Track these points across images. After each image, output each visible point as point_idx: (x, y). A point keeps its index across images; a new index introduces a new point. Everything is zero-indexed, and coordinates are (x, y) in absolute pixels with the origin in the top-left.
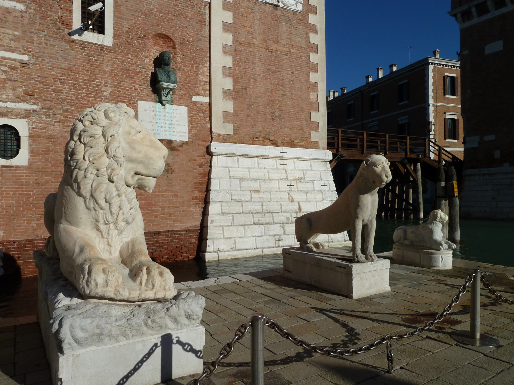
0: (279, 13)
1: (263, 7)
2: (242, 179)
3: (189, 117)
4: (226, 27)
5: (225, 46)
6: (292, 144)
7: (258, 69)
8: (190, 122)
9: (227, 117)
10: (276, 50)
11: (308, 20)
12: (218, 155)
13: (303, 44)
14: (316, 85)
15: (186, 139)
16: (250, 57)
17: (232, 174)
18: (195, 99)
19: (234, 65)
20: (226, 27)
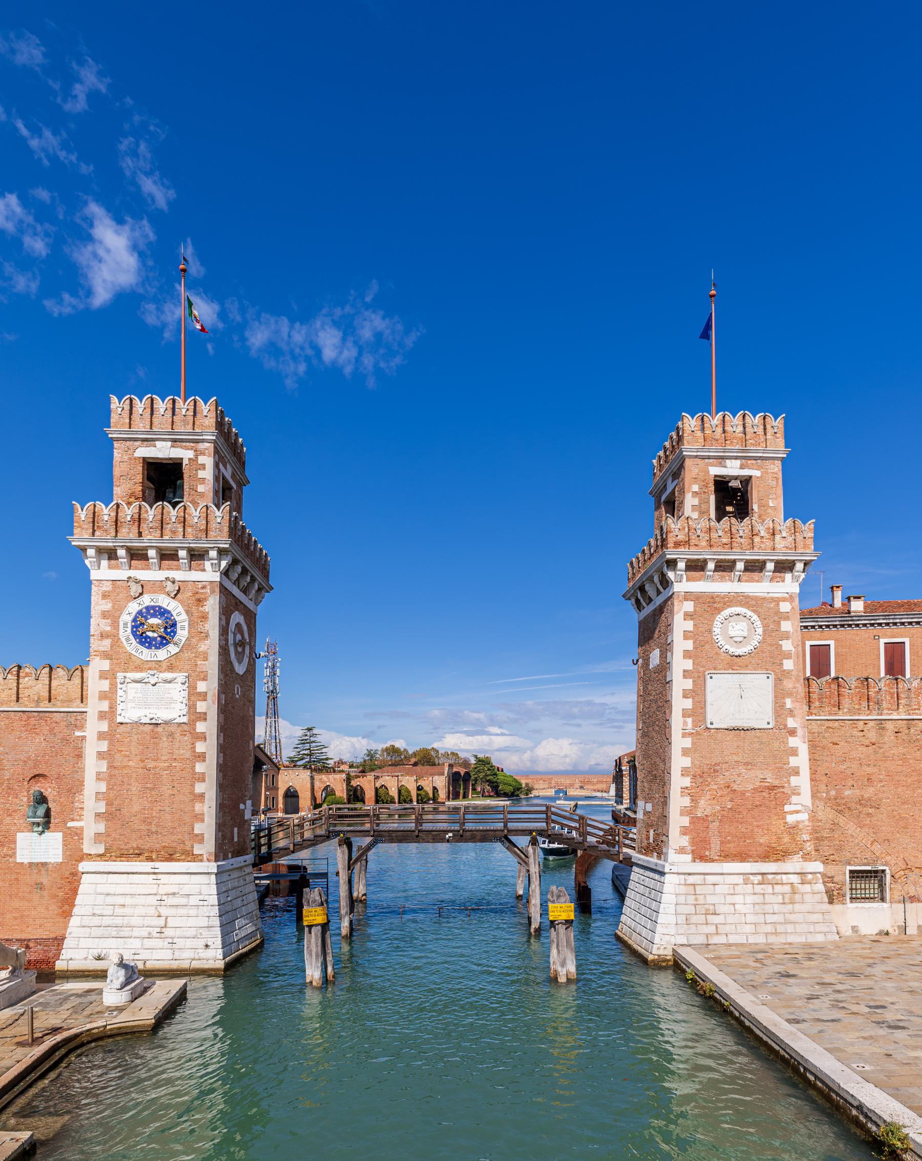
0: (160, 729)
1: (141, 728)
2: (108, 894)
3: (64, 841)
4: (100, 755)
5: (98, 774)
6: (170, 858)
7: (134, 789)
8: (65, 845)
9: (98, 837)
10: (155, 767)
11: (194, 729)
12: (87, 873)
13: (188, 755)
14: (202, 796)
15: (60, 860)
16: (125, 780)
17: (99, 890)
18: (70, 824)
19: (108, 789)
20: (100, 755)
